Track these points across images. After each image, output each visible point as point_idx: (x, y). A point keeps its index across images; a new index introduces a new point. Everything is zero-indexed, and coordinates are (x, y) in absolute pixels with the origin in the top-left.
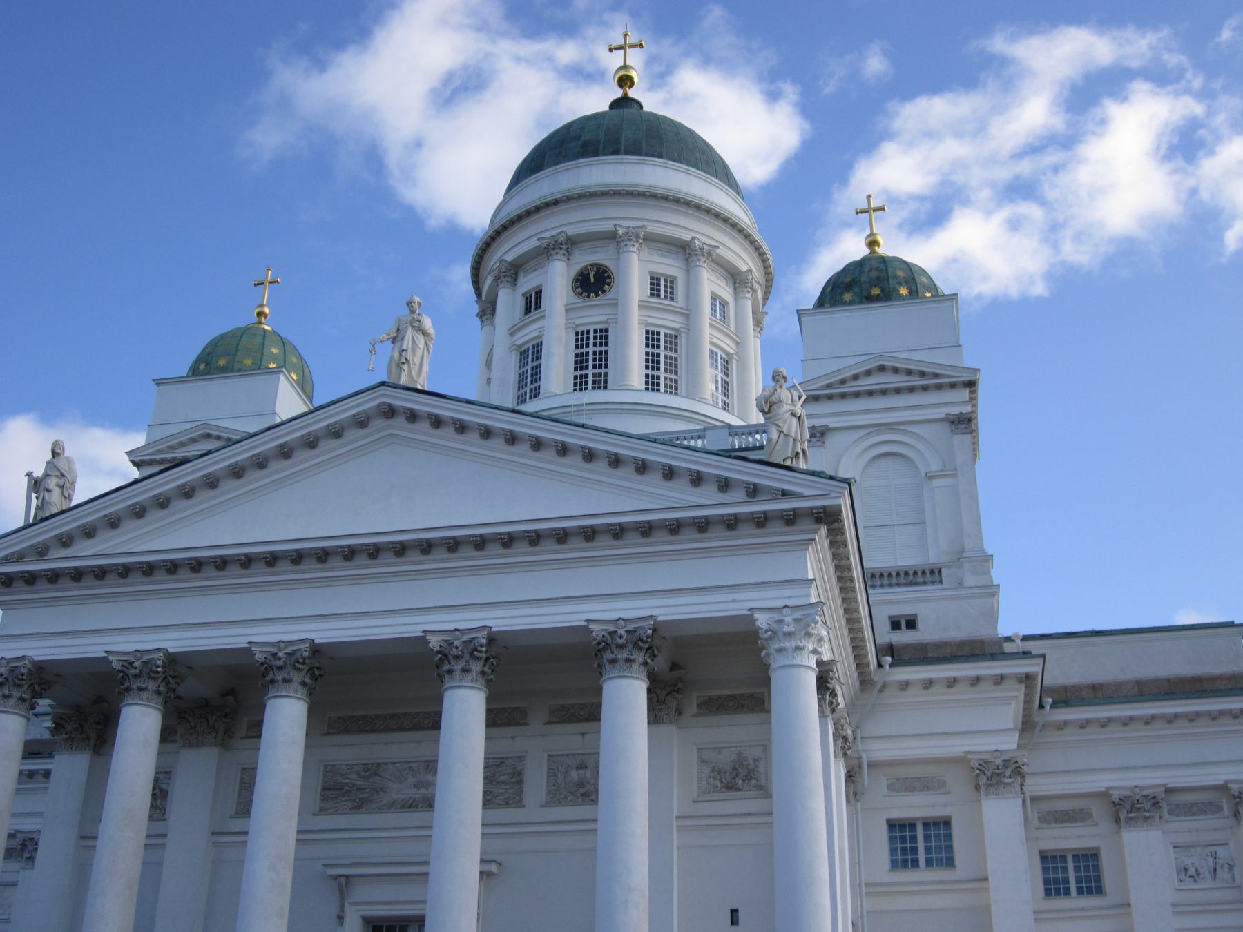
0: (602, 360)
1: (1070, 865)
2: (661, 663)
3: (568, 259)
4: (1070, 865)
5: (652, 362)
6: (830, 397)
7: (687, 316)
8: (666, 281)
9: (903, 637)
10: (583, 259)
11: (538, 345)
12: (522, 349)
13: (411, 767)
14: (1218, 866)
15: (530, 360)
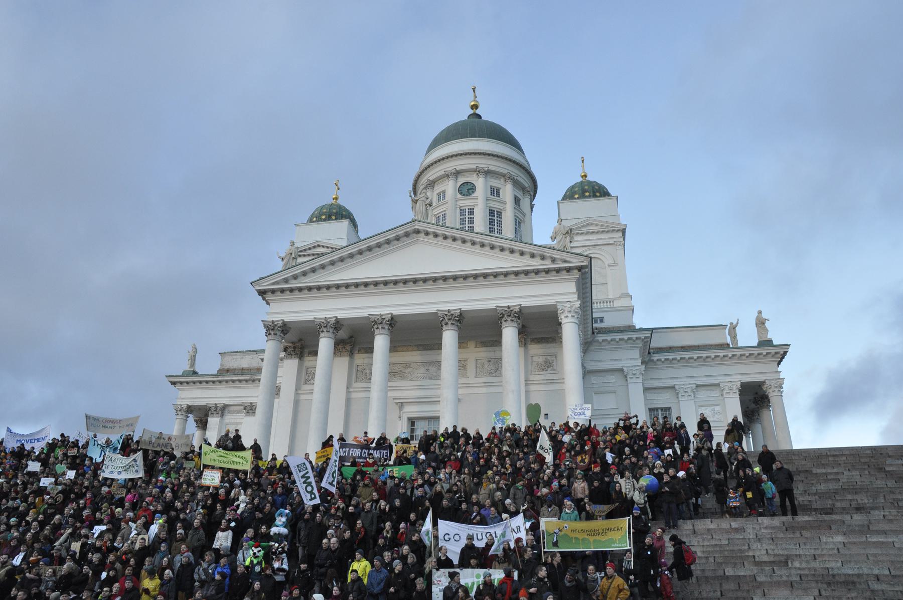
0: (472, 221)
5: (491, 222)
7: (506, 204)
8: (497, 190)
10: (462, 180)
12: (437, 216)
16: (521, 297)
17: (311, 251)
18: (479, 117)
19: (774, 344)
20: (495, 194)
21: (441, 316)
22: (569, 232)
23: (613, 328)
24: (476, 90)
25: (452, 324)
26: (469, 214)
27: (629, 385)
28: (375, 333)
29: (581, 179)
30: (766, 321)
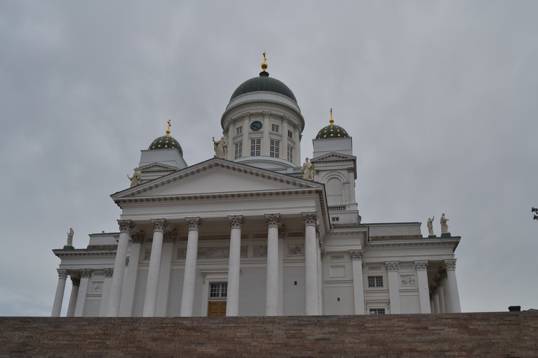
0: (259, 147)
1: (375, 279)
2: (280, 224)
3: (250, 119)
4: (375, 279)
5: (272, 148)
6: (320, 162)
7: (282, 137)
8: (276, 126)
9: (335, 222)
10: (254, 120)
11: (241, 143)
13: (220, 248)
14: (411, 281)
15: (239, 146)
16: (280, 208)
17: (151, 169)
18: (267, 74)
19: (452, 236)
20: (275, 129)
21: (231, 220)
22: (313, 167)
23: (345, 224)
24: (265, 55)
25: (237, 225)
26: (257, 143)
27: (353, 262)
28: (189, 230)
29: (330, 124)
30: (447, 221)
